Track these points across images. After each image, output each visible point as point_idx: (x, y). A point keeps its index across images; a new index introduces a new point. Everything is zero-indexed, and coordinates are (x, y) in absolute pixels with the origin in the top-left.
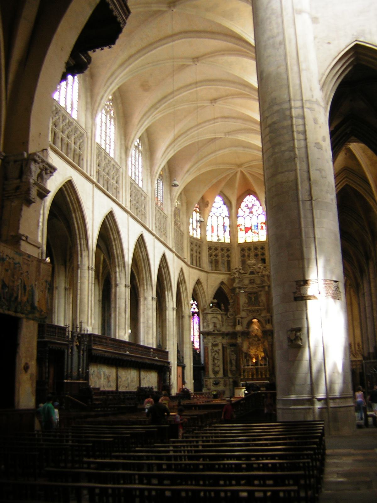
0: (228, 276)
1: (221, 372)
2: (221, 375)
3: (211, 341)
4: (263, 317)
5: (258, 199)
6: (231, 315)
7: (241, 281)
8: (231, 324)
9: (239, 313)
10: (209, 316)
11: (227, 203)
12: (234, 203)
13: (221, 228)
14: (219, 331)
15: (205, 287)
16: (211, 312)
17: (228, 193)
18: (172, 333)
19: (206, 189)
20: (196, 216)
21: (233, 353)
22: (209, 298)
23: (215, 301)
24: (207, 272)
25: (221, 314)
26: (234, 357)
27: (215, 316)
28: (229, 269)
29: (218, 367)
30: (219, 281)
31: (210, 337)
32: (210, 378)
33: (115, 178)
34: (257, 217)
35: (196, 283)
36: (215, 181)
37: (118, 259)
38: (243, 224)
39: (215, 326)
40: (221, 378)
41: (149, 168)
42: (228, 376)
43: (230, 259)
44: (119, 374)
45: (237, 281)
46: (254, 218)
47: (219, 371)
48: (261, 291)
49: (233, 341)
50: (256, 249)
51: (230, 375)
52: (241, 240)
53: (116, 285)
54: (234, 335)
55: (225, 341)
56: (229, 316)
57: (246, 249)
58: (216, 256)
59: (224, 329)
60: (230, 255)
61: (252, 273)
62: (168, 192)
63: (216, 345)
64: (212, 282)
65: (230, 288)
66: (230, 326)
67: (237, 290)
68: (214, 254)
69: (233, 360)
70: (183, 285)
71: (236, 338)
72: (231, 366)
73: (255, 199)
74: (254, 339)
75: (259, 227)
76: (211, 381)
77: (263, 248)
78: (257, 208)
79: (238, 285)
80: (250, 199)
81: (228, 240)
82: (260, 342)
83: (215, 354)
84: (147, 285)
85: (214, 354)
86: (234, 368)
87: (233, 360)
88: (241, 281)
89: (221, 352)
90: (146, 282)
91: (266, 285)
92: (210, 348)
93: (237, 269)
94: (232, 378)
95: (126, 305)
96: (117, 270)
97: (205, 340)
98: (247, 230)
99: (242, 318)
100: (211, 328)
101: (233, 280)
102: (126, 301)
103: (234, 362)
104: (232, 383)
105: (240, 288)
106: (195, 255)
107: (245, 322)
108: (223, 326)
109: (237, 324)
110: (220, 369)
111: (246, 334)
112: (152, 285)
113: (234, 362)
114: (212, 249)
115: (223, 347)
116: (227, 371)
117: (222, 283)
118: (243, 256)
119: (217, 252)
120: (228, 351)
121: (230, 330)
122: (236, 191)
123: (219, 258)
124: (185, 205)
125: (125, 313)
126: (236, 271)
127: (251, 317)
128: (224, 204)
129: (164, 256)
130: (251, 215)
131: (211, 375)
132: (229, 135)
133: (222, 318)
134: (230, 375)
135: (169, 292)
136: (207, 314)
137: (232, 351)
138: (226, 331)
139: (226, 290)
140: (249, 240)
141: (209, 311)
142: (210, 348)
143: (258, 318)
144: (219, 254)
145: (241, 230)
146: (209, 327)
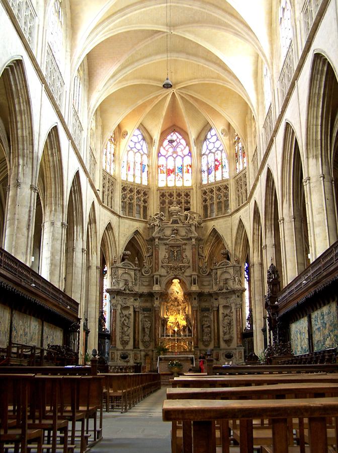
0: (144, 224)
1: (131, 343)
2: (130, 346)
3: (121, 302)
4: (186, 276)
5: (185, 134)
6: (147, 272)
7: (162, 230)
8: (146, 284)
9: (157, 270)
10: (120, 272)
11: (147, 138)
12: (156, 136)
13: (138, 167)
14: (131, 291)
15: (116, 235)
16: (122, 267)
17: (149, 127)
18: (79, 282)
19: (129, 111)
20: (111, 147)
22: (120, 249)
23: (128, 252)
24: (119, 216)
25: (135, 270)
26: (148, 325)
27: (127, 272)
28: (145, 216)
29: (128, 336)
30: (133, 230)
31: (119, 298)
32: (117, 350)
33: (29, 25)
34: (183, 158)
35: (106, 228)
36: (140, 102)
37: (23, 145)
38: (165, 165)
39: (126, 284)
40: (130, 350)
41: (69, 50)
42: (139, 348)
43: (146, 204)
44: (14, 322)
45: (157, 229)
46: (179, 159)
48: (185, 244)
49: (148, 305)
50: (179, 195)
51: (141, 347)
52: (162, 184)
53: (18, 185)
54: (151, 295)
55: (137, 304)
56: (144, 274)
57: (167, 194)
58: (131, 199)
59: (137, 289)
60: (146, 200)
61: (175, 222)
62: (86, 99)
63: (127, 308)
64: (125, 229)
65: (148, 238)
66: (146, 286)
67: (157, 240)
68: (128, 196)
69: (147, 327)
70: (93, 225)
71: (152, 301)
72: (144, 336)
73: (180, 137)
74: (173, 303)
75: (185, 171)
76: (119, 353)
77: (187, 195)
78: (183, 148)
79: (157, 235)
80: (174, 136)
81: (145, 183)
82: (180, 307)
83: (125, 320)
84: (56, 204)
85: (123, 319)
86: (147, 338)
88: (162, 230)
89: (132, 317)
90: (56, 200)
91: (194, 237)
92: (119, 311)
93: (159, 215)
94: (144, 351)
95: (29, 216)
96: (21, 162)
97: (114, 301)
98: (170, 172)
99: (160, 276)
100: (121, 286)
101: (153, 227)
102: (30, 211)
103: (147, 331)
104: (143, 358)
105: (160, 239)
106: (106, 193)
107: (164, 281)
108: (136, 285)
109: (155, 283)
111: (164, 296)
112: (63, 206)
113: (147, 331)
114: (126, 190)
115: (135, 312)
116: (138, 342)
117: (137, 232)
118: (163, 203)
119: (132, 194)
120: (141, 317)
121: (145, 290)
122: (162, 121)
123: (135, 201)
124: (100, 128)
125: (28, 229)
126: (156, 218)
127: (172, 275)
128: (144, 139)
129: (77, 173)
130: (175, 155)
131: (119, 346)
132: (174, 30)
133: (135, 274)
134: (141, 347)
135: (79, 228)
136: (117, 267)
138: (140, 291)
139: (141, 242)
140: (171, 184)
141: (120, 265)
142: (119, 311)
143: (180, 277)
144: (134, 199)
145: (162, 172)
146: (119, 285)
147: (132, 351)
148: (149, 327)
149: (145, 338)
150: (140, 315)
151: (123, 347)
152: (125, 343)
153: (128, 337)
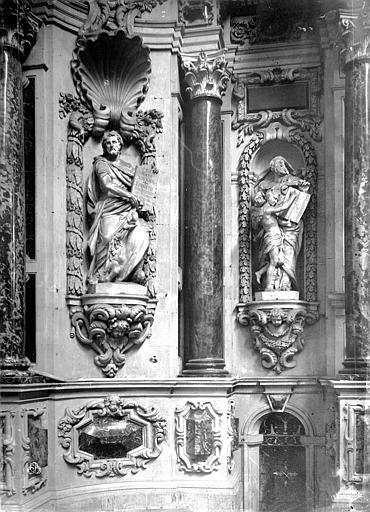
21: (279, 163)
29: (131, 278)
32: (49, 390)
47: (144, 320)
72: (259, 286)
86: (280, 296)
87: (280, 217)
89: (167, 142)
94: (260, 389)
103: (282, 246)
110: (151, 297)
113: (282, 246)
115: (188, 102)
116: (218, 324)
120: (236, 146)
137: (265, 151)
147: (171, 390)
148: (295, 215)
149: (266, 296)
150: (231, 138)
151: (102, 365)
152: (108, 335)
153: (133, 289)
